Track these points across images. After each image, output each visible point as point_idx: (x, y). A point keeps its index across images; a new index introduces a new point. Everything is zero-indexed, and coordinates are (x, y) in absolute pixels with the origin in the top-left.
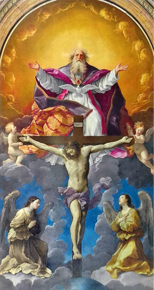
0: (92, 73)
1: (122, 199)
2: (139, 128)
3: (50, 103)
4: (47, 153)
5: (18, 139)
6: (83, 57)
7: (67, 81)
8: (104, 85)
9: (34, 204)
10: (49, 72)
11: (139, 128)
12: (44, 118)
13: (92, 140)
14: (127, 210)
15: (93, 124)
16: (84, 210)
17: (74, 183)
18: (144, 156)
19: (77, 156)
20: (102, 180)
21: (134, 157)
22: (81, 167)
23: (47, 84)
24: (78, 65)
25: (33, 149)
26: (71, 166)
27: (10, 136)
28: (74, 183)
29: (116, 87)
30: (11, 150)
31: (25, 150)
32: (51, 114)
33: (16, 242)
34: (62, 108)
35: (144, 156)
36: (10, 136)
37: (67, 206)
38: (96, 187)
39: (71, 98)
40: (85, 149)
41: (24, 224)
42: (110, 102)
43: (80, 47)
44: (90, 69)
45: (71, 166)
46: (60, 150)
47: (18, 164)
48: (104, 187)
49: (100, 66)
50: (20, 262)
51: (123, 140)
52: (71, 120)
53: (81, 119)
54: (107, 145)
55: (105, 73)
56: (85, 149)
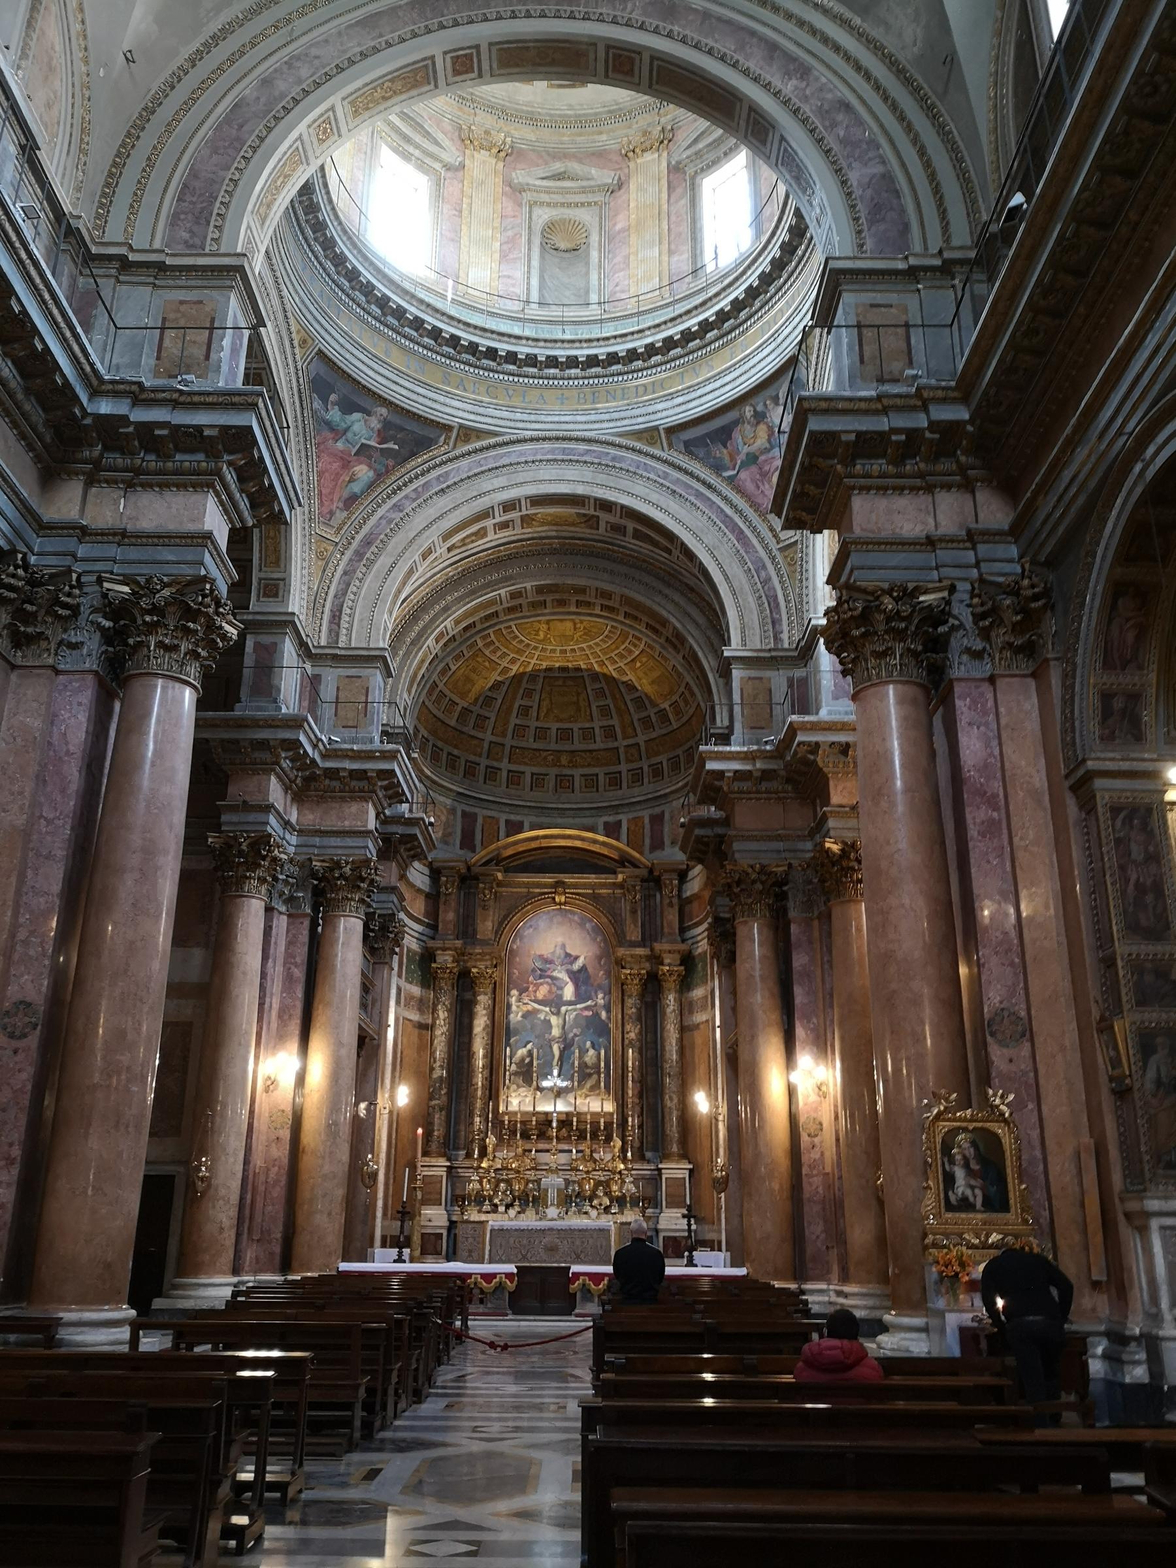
0: (570, 958)
1: (588, 1044)
2: (600, 996)
3: (541, 977)
4: (538, 1011)
5: (519, 1000)
6: (563, 946)
7: (551, 962)
8: (576, 966)
9: (529, 1046)
10: (541, 956)
11: (600, 996)
12: (537, 986)
13: (570, 1003)
14: (591, 1052)
15: (569, 992)
16: (562, 1052)
17: (556, 1032)
18: (604, 1015)
19: (558, 1013)
20: (575, 1031)
21: (597, 1015)
22: (561, 1021)
23: (539, 964)
24: (559, 951)
25: (529, 1008)
26: (554, 1020)
27: (514, 999)
28: (556, 1032)
29: (583, 969)
30: (514, 1008)
31: (525, 1008)
32: (542, 984)
33: (516, 1074)
34: (549, 980)
35: (604, 1015)
36: (514, 999)
37: (551, 1047)
38: (571, 1035)
39: (555, 974)
40: (563, 1009)
41: (523, 1060)
42: (580, 978)
43: (560, 940)
44: (568, 955)
45: (554, 1020)
46: (547, 1009)
47: (519, 1018)
48: (576, 1035)
49: (573, 953)
50: (519, 1087)
51: (589, 1003)
52: (554, 989)
53: (561, 989)
54: (578, 1006)
55: (577, 958)
56: (563, 1009)
